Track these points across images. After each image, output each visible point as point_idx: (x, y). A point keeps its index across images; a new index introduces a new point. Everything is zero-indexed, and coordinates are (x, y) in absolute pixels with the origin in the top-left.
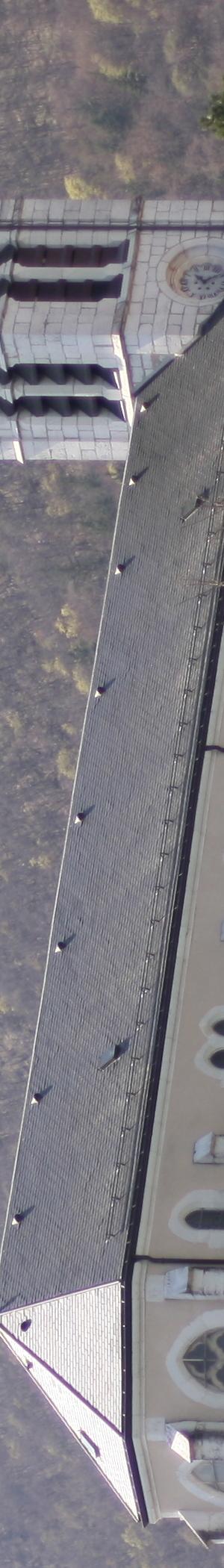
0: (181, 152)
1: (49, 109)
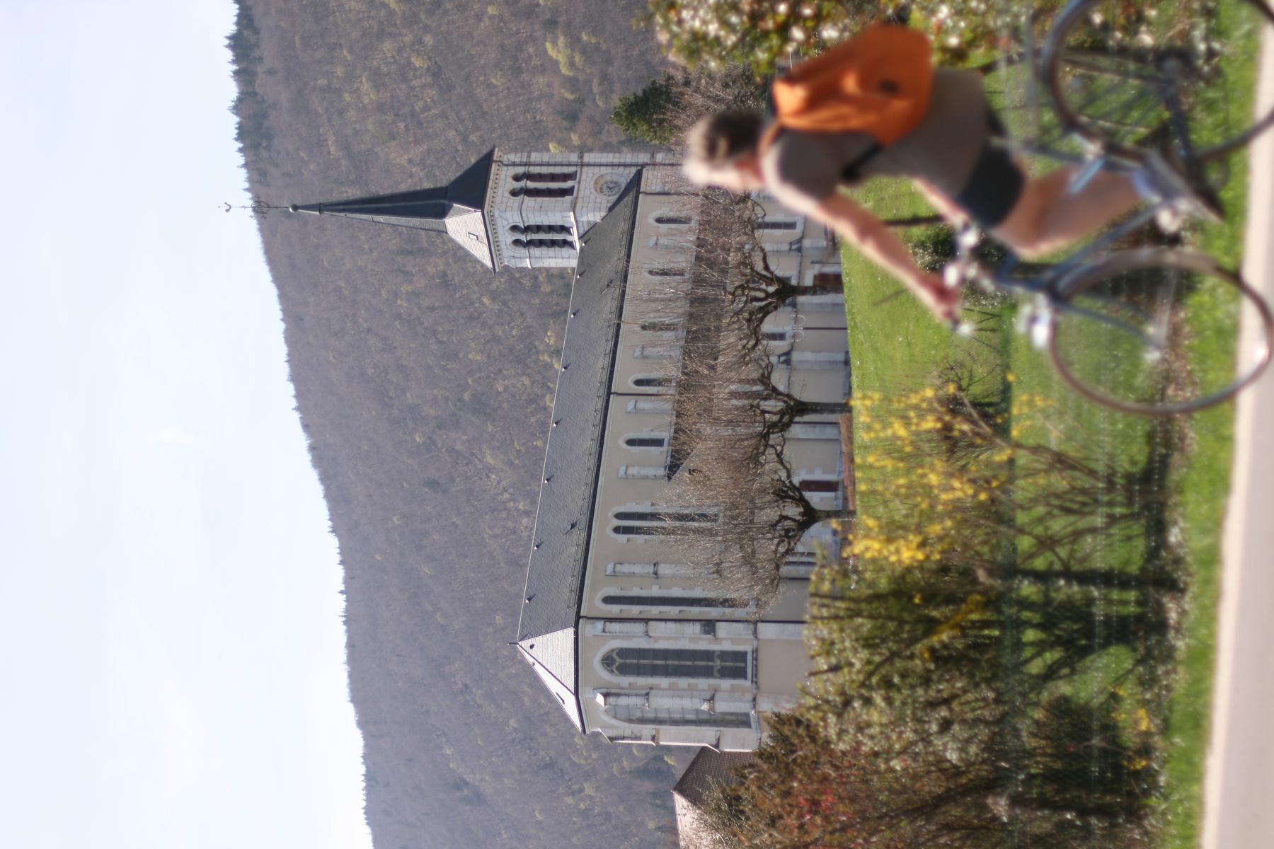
0: (600, 132)
1: (542, 113)
